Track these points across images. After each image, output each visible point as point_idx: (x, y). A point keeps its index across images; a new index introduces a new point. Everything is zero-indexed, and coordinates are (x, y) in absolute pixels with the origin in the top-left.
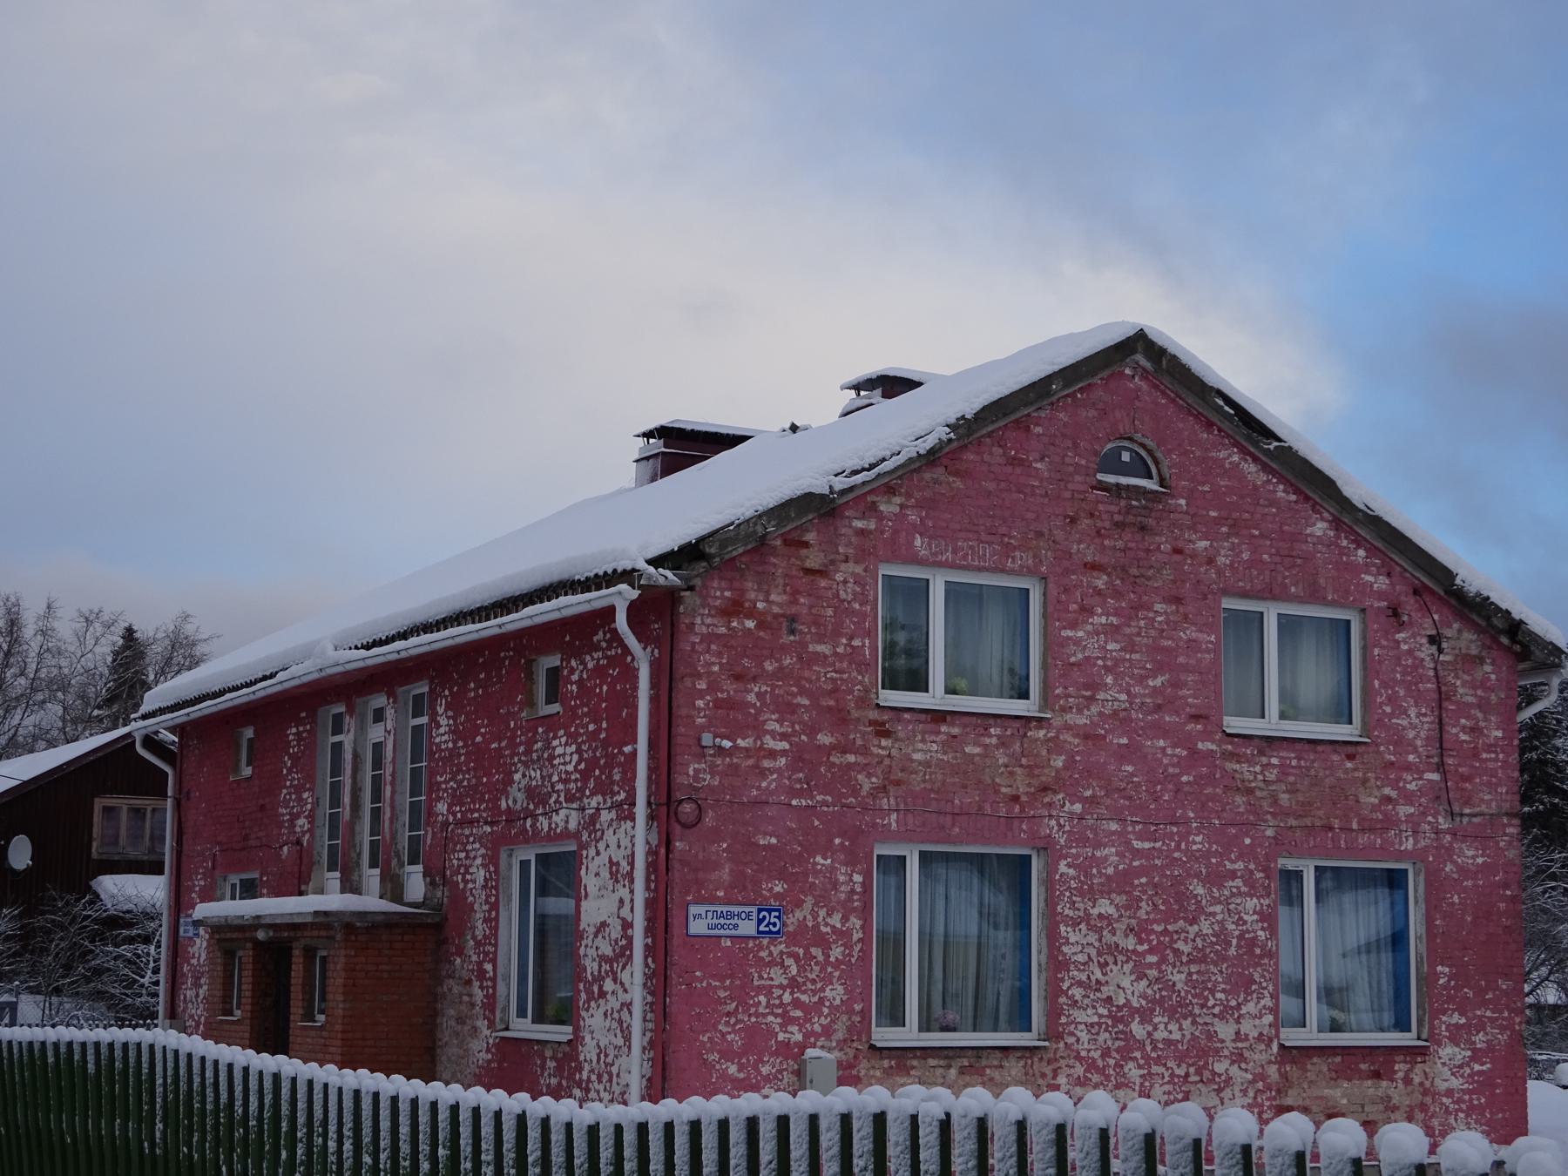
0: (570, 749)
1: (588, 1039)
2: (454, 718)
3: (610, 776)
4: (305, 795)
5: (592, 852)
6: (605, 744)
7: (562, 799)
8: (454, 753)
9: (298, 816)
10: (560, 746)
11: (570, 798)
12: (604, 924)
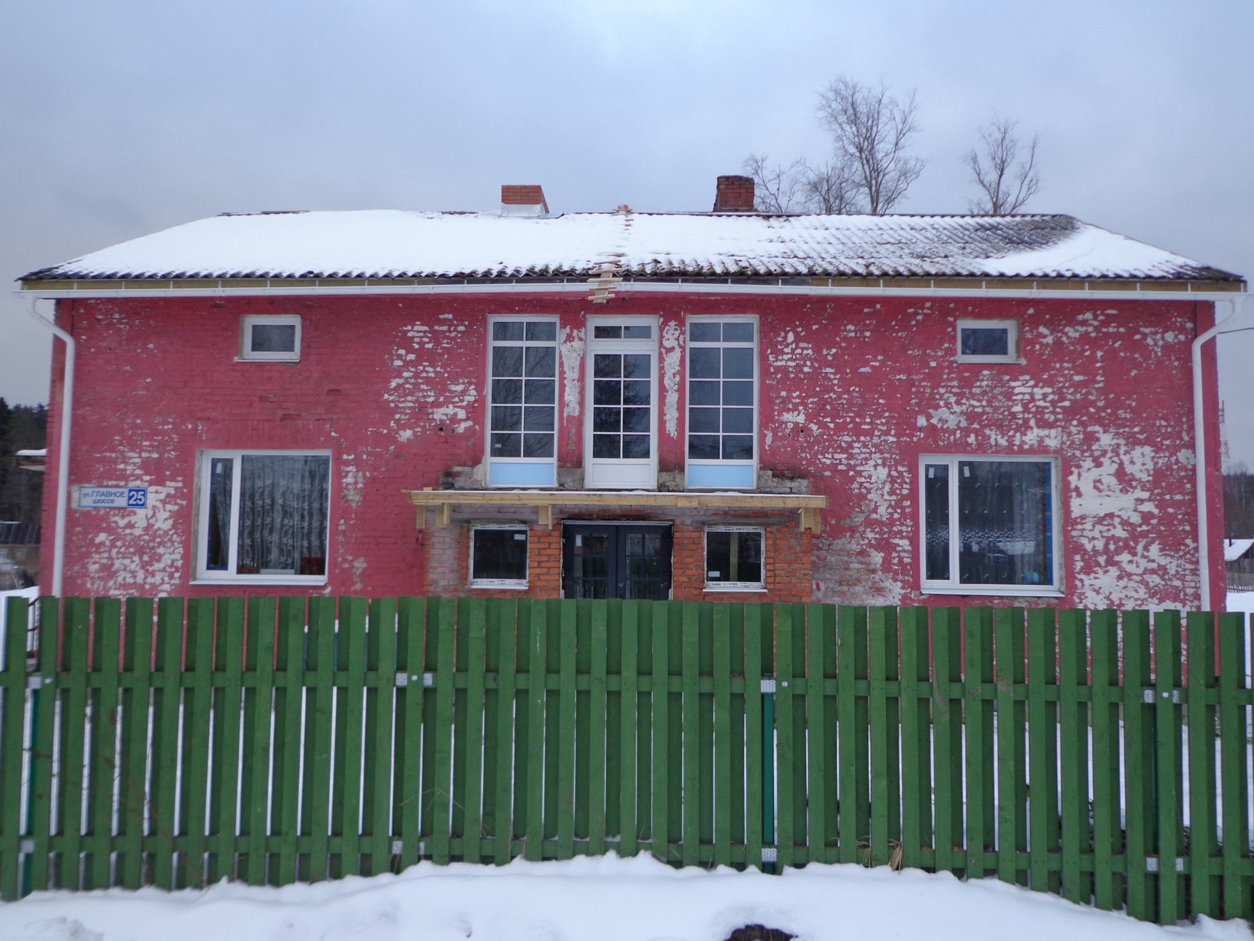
0: (1036, 390)
1: (1090, 593)
2: (818, 350)
3: (1114, 413)
4: (460, 388)
5: (1088, 463)
6: (1104, 392)
7: (1032, 423)
8: (814, 377)
9: (437, 405)
10: (1021, 388)
11: (1043, 424)
12: (1111, 516)
